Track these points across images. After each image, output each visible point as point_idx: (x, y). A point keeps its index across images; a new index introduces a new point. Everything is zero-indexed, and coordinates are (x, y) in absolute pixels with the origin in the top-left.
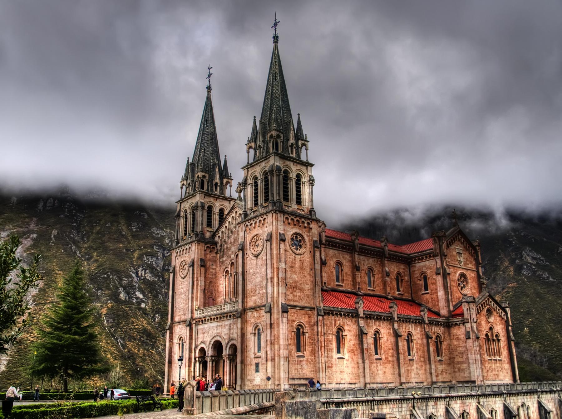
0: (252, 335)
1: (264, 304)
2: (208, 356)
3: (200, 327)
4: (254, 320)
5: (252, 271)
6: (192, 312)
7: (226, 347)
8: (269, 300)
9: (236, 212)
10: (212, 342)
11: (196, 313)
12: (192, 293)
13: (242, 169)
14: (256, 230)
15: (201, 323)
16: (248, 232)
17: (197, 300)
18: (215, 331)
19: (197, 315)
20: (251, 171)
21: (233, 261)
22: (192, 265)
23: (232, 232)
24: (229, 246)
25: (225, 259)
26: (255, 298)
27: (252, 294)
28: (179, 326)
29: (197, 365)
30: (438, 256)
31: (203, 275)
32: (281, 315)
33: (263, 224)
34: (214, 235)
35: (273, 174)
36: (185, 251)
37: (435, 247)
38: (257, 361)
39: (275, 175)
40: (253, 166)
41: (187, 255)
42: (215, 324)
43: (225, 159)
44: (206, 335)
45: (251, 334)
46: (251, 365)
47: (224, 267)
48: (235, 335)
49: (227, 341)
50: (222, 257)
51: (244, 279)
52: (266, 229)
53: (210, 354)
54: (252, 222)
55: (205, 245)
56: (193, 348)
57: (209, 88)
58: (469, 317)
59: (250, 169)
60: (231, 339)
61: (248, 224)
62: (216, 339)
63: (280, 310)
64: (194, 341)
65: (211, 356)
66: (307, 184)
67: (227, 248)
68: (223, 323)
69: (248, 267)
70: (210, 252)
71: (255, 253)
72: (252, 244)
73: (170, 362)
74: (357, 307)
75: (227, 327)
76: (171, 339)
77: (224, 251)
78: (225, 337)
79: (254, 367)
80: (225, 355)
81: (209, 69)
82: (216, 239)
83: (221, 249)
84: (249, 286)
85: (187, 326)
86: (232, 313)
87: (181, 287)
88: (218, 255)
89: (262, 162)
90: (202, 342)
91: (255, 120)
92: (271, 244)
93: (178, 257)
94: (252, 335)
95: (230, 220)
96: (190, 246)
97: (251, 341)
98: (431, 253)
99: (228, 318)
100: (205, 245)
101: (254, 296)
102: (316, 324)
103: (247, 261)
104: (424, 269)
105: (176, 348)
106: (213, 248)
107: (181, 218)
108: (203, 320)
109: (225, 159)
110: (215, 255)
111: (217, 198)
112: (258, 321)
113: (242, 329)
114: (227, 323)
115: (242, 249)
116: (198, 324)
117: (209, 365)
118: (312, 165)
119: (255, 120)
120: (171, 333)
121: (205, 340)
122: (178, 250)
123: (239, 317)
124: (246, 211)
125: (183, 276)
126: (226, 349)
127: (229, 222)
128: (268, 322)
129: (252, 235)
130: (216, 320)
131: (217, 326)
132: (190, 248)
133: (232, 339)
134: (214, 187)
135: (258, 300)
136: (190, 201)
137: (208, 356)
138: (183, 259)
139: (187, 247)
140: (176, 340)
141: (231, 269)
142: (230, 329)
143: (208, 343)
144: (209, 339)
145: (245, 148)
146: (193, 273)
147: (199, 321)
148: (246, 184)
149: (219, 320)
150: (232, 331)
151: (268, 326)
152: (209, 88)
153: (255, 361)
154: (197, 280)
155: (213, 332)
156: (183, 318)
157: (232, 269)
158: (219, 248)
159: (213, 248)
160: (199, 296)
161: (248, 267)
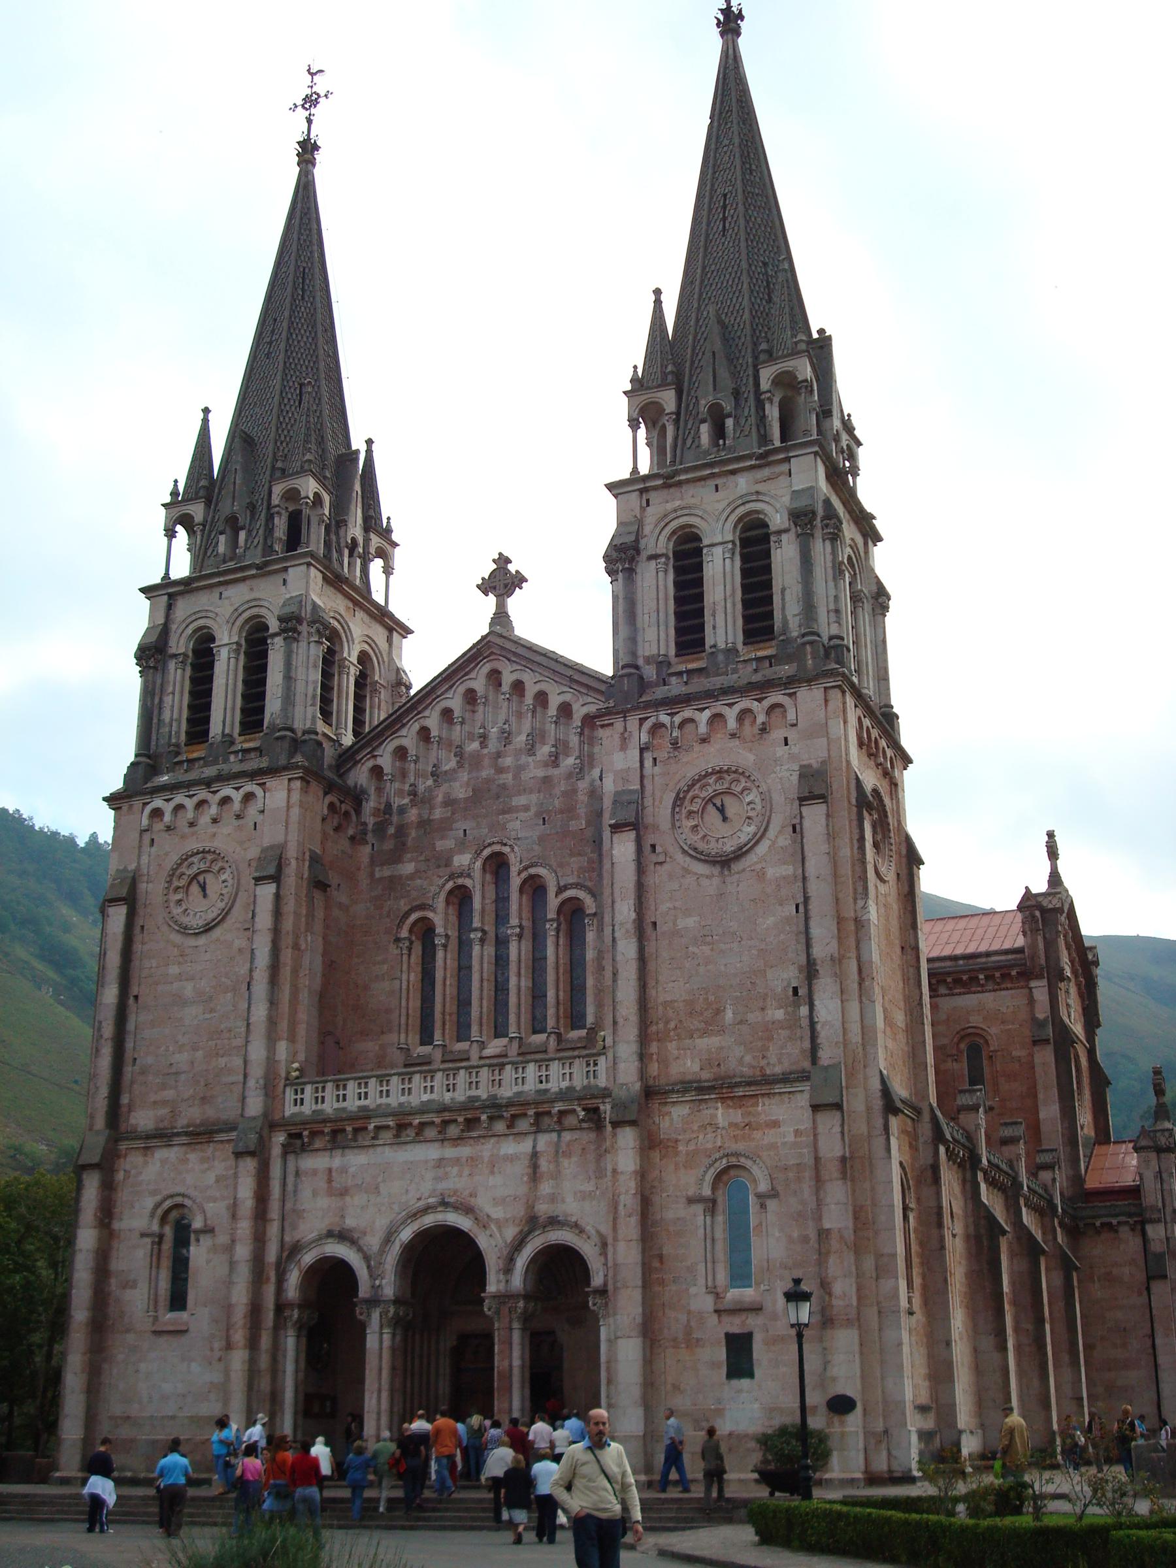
0: (699, 1209)
1: (778, 1070)
2: (373, 1302)
3: (316, 1162)
4: (708, 1141)
5: (691, 922)
6: (270, 1090)
7: (511, 1260)
8: (826, 1056)
9: (495, 677)
10: (406, 1235)
11: (290, 1094)
12: (273, 1003)
13: (611, 487)
14: (712, 749)
15: (318, 1144)
16: (662, 755)
17: (292, 1039)
18: (427, 1186)
19: (301, 1105)
20: (662, 503)
21: (468, 882)
22: (276, 878)
23: (460, 754)
24: (438, 814)
25: (408, 868)
26: (714, 1041)
27: (695, 1024)
28: (161, 1154)
29: (290, 1342)
30: (1039, 977)
31: (318, 927)
32: (879, 1123)
33: (764, 730)
34: (347, 758)
35: (813, 527)
36: (214, 810)
37: (1033, 946)
38: (735, 1325)
39: (818, 533)
40: (679, 484)
41: (228, 827)
42: (429, 1152)
43: (369, 452)
44: (356, 1201)
45: (691, 1201)
46: (691, 1342)
47: (403, 905)
48: (571, 1207)
49: (510, 1233)
50: (395, 857)
51: (642, 959)
52: (781, 751)
53: (389, 1291)
54: (687, 713)
55: (326, 794)
56: (271, 1255)
57: (307, 150)
58: (1160, 1204)
59: (653, 496)
60: (533, 1223)
61: (664, 719)
62: (429, 1220)
63: (878, 1103)
64: (273, 1230)
65: (397, 1301)
66: (867, 606)
67: (423, 824)
68: (486, 1149)
69: (664, 907)
70: (337, 829)
71: (713, 848)
72: (688, 806)
73: (100, 1325)
74: (972, 1128)
75: (521, 1168)
76: (107, 1214)
77: (401, 831)
78: (497, 1213)
79: (722, 1354)
80: (503, 1298)
81: (312, 75)
82: (360, 776)
83: (380, 828)
84: (671, 989)
85: (238, 1155)
86: (558, 1107)
87: (174, 970)
88: (367, 849)
89: (733, 472)
90: (330, 1234)
91: (658, 303)
92: (828, 816)
93: (163, 839)
94: (699, 1209)
95: (454, 701)
96: (250, 787)
97: (694, 1239)
98: (1012, 966)
99: (523, 1125)
100: (326, 794)
101: (705, 1033)
102: (929, 1173)
103: (656, 877)
104: (975, 1020)
105: (134, 1258)
106: (347, 814)
107: (172, 665)
108: (342, 1132)
109: (369, 452)
110: (345, 844)
111: (356, 603)
112: (740, 1147)
113: (642, 1175)
114: (510, 1147)
115: (633, 823)
116: (304, 1149)
117: (378, 1341)
118: (877, 538)
119: (658, 303)
120: (108, 1187)
121: (350, 1222)
122: (158, 803)
123: (633, 1123)
124: (637, 667)
125: (196, 922)
126: (508, 1270)
127: (447, 713)
128: (832, 1147)
129: (691, 773)
130: (431, 1133)
131: (440, 1163)
132: (249, 797)
133: (554, 1222)
134: (346, 552)
135: (738, 1051)
136: (238, 594)
137: (373, 1302)
138: (193, 845)
139: (227, 791)
140: (137, 1217)
141: (446, 914)
142: (535, 1174)
143: (373, 1242)
144: (382, 1223)
145: (622, 407)
146: (277, 913)
147: (314, 1134)
148: (638, 552)
149: (453, 1131)
150: (546, 1188)
151: (831, 1170)
152: (307, 150)
153: (716, 1330)
154: (296, 947)
155: (425, 1188)
156: (191, 1114)
157: (453, 918)
158: (371, 821)
159: (347, 814)
160: (302, 1016)
161: (661, 907)
